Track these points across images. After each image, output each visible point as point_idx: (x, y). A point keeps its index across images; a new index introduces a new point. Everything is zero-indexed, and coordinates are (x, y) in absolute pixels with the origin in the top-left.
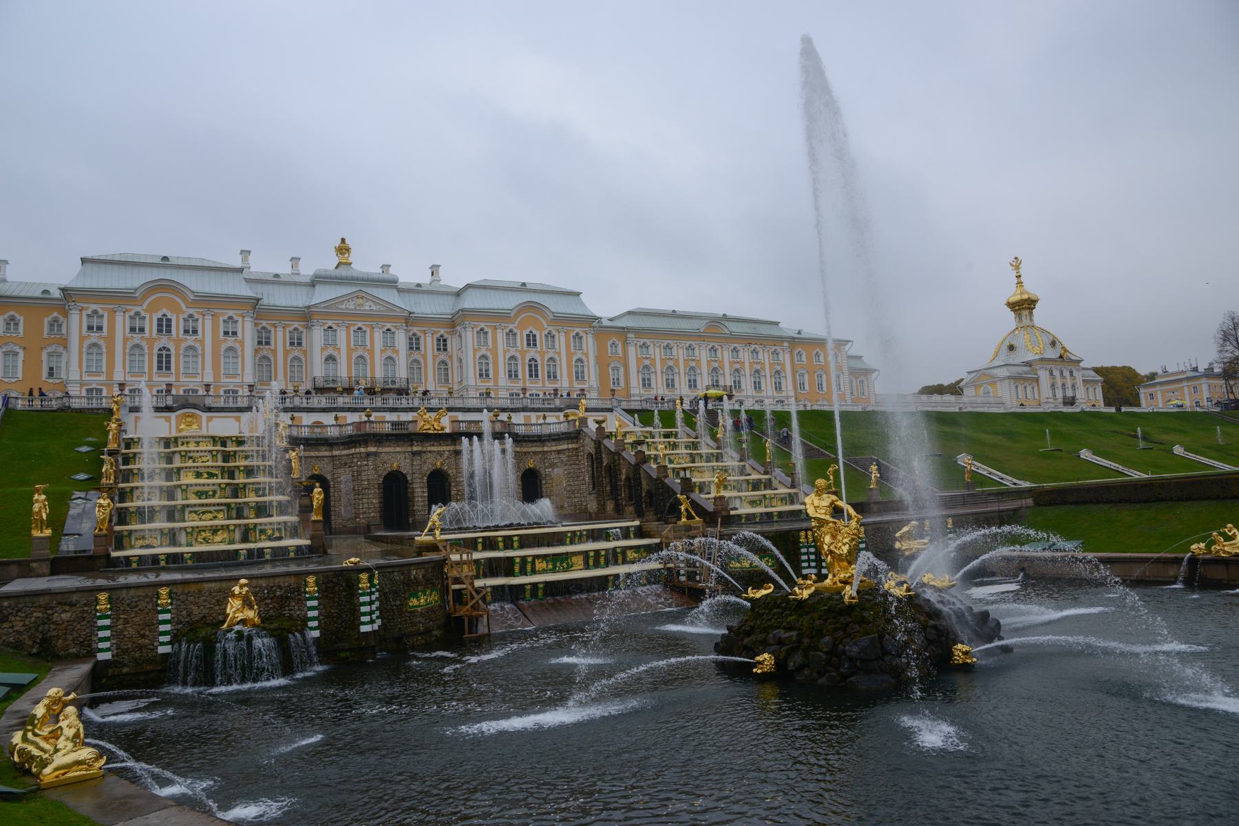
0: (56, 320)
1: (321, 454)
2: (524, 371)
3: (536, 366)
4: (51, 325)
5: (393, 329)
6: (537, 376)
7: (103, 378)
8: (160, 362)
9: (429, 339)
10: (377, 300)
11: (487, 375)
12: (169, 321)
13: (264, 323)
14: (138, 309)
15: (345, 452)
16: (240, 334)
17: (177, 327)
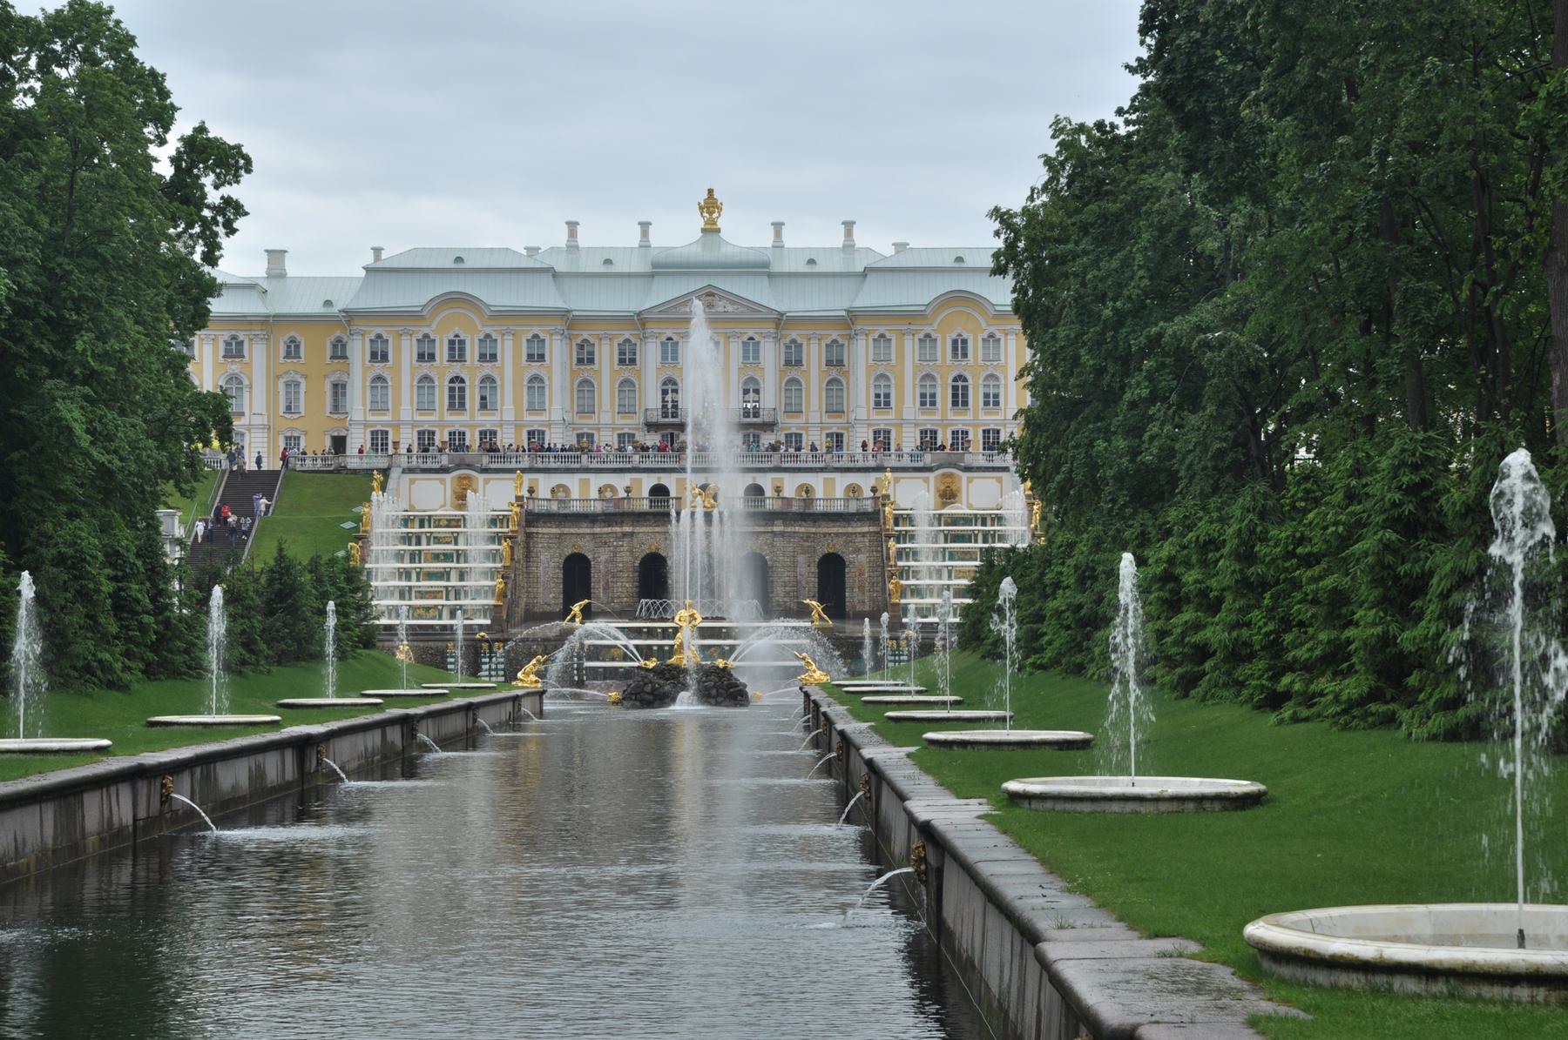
0: (339, 340)
1: (582, 531)
2: (944, 395)
3: (965, 388)
4: (335, 346)
5: (757, 338)
6: (965, 403)
7: (387, 418)
8: (452, 397)
9: (814, 348)
10: (734, 299)
11: (887, 404)
12: (462, 342)
13: (586, 337)
14: (426, 330)
15: (606, 530)
16: (547, 358)
17: (472, 351)
